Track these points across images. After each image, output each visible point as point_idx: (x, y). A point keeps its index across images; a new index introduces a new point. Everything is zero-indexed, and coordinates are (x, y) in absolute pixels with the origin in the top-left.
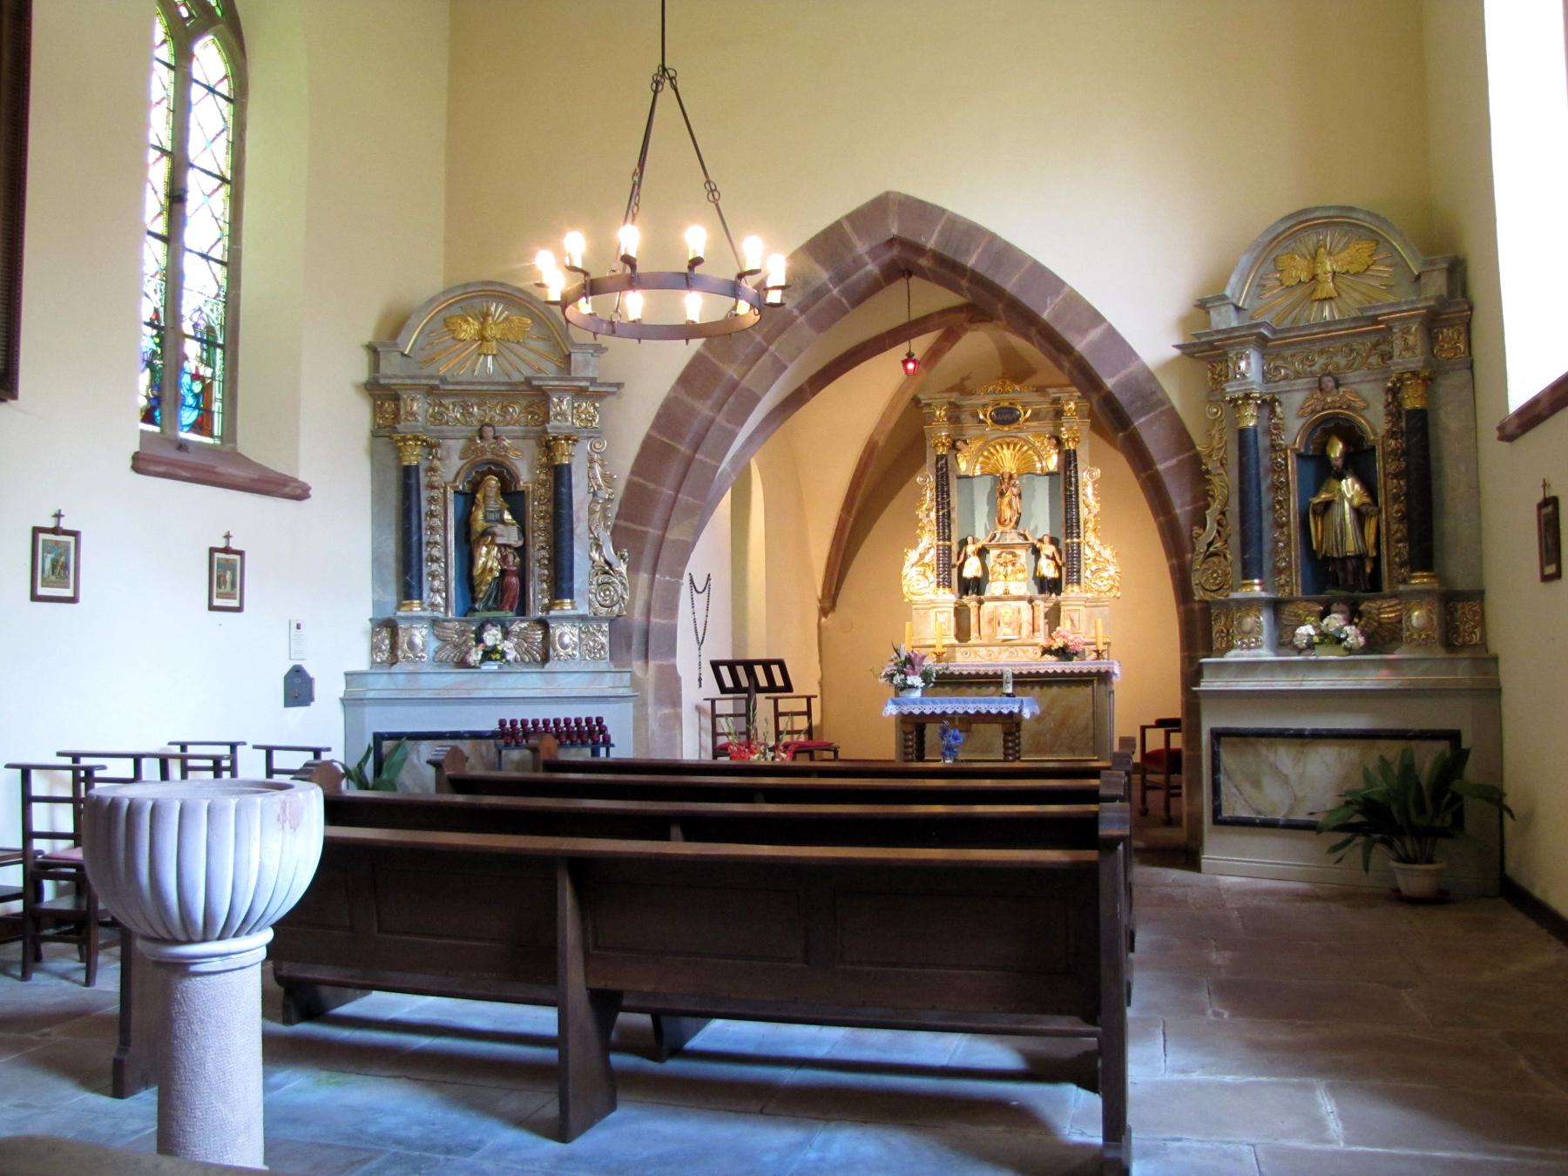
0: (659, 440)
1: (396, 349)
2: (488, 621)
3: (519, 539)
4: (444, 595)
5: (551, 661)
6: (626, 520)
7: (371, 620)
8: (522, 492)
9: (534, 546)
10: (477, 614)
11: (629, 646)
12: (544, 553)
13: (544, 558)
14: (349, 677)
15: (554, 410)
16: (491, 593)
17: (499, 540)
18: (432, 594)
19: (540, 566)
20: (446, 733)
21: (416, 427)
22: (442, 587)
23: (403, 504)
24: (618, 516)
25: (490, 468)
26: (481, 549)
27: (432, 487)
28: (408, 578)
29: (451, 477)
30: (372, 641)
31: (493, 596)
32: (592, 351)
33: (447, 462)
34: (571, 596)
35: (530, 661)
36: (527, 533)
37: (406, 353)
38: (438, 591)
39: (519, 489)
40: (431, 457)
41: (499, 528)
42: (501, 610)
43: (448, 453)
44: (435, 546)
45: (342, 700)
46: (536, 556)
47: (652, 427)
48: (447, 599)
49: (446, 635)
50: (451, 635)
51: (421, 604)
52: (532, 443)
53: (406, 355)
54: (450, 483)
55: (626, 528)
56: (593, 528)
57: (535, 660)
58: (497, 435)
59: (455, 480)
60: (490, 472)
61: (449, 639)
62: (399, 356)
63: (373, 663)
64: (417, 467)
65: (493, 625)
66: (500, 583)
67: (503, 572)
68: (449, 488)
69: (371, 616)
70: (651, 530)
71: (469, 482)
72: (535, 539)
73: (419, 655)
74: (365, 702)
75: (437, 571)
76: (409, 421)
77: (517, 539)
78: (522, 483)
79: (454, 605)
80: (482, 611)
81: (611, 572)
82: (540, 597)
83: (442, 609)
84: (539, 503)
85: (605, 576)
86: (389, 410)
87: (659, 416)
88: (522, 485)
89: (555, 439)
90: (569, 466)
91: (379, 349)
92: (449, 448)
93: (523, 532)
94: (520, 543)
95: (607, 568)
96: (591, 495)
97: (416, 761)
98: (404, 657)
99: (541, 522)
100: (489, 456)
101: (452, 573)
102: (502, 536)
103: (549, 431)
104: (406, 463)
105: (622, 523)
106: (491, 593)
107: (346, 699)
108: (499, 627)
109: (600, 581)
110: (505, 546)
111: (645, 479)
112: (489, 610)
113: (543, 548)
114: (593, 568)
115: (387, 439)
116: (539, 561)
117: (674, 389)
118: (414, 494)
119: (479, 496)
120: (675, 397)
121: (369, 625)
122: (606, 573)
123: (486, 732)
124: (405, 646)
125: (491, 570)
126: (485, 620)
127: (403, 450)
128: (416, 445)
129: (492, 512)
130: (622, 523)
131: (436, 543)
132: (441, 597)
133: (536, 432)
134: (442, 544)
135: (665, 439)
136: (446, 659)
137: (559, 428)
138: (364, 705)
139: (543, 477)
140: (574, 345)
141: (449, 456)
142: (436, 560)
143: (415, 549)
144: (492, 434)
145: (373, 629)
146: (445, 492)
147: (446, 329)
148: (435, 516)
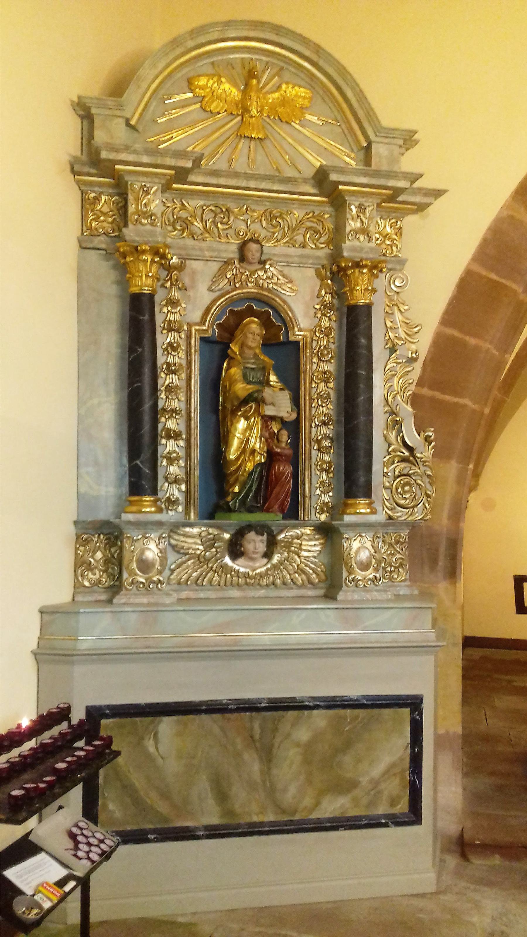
0: (485, 277)
1: (118, 113)
2: (249, 527)
3: (292, 411)
4: (183, 487)
5: (344, 587)
6: (430, 388)
7: (76, 523)
8: (297, 343)
9: (311, 421)
10: (233, 515)
11: (434, 561)
12: (325, 430)
13: (326, 437)
14: (46, 617)
15: (352, 224)
16: (251, 487)
17: (269, 411)
18: (166, 484)
19: (319, 449)
20: (201, 703)
21: (152, 234)
22: (181, 474)
23: (131, 350)
24: (420, 383)
25: (250, 307)
26: (238, 421)
27: (171, 328)
28: (138, 462)
29: (197, 316)
30: (76, 554)
31: (254, 488)
32: (401, 142)
33: (191, 293)
34: (368, 494)
35: (303, 584)
36: (302, 402)
37: (133, 123)
38: (176, 481)
39: (292, 338)
40: (168, 284)
41: (267, 393)
42: (267, 511)
43: (193, 281)
44: (172, 416)
45: (35, 654)
46: (313, 434)
47: (475, 259)
48: (188, 493)
49: (186, 545)
50: (194, 546)
51: (155, 503)
52: (311, 272)
53: (133, 128)
54: (196, 324)
55: (433, 399)
56: (390, 398)
57: (310, 582)
58: (264, 258)
59: (203, 322)
60: (250, 312)
61: (190, 551)
62: (123, 126)
63: (78, 587)
64: (151, 297)
65: (257, 533)
66: (264, 473)
67: (271, 456)
68: (193, 331)
69: (75, 518)
70: (466, 401)
71: (219, 326)
72: (314, 411)
73: (155, 579)
74: (75, 658)
75: (175, 452)
76: (141, 223)
77: (290, 410)
78: (296, 329)
79: (198, 502)
80: (239, 511)
81: (411, 458)
82: (318, 492)
83: (180, 509)
84: (320, 360)
85: (403, 465)
86: (105, 209)
87: (485, 243)
88: (297, 335)
89: (357, 265)
90: (368, 307)
91: (93, 111)
92: (194, 272)
93: (296, 401)
94: (294, 416)
95: (407, 454)
96: (388, 351)
97: (152, 749)
98: (132, 583)
99: (322, 386)
100: (251, 289)
101: (196, 454)
102: (273, 404)
103: (345, 254)
104: (134, 290)
105: (425, 391)
106: (251, 487)
107: (38, 654)
108: (265, 537)
109: (397, 473)
110: (273, 418)
111: (461, 330)
112: (251, 510)
113: (324, 423)
114: (389, 454)
115: (104, 252)
116: (319, 442)
117: (507, 206)
118: (147, 335)
119: (235, 348)
120: (511, 217)
121: (72, 530)
122: (404, 460)
123: (259, 701)
124: (134, 565)
125: (253, 452)
126: (244, 524)
127: (132, 266)
128: (153, 261)
129: (252, 369)
130: (425, 391)
131: (174, 411)
132: (179, 490)
133: (318, 258)
134: (183, 412)
135: (493, 276)
136: (187, 581)
137: (360, 249)
138: (73, 663)
139: (326, 323)
140: (379, 129)
141: (193, 285)
142: (177, 436)
143: (147, 418)
144: (258, 255)
145: (78, 537)
146: (189, 337)
147: (190, 95)
148: (174, 372)
